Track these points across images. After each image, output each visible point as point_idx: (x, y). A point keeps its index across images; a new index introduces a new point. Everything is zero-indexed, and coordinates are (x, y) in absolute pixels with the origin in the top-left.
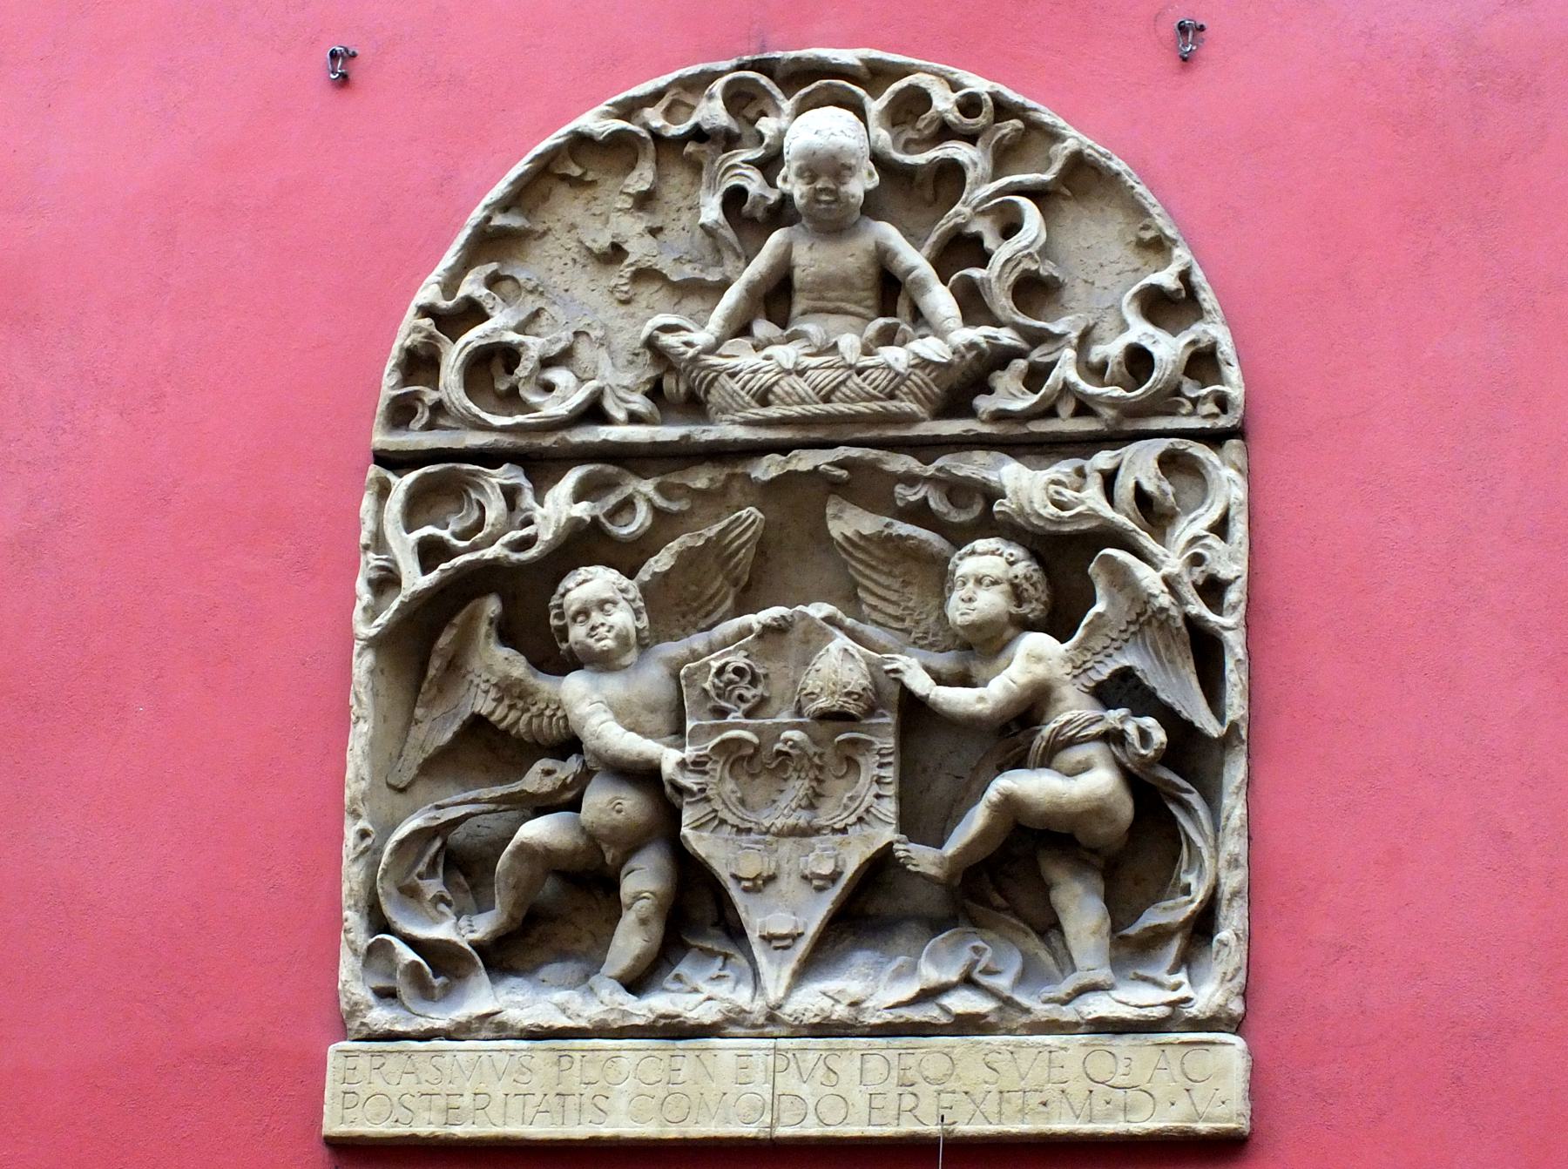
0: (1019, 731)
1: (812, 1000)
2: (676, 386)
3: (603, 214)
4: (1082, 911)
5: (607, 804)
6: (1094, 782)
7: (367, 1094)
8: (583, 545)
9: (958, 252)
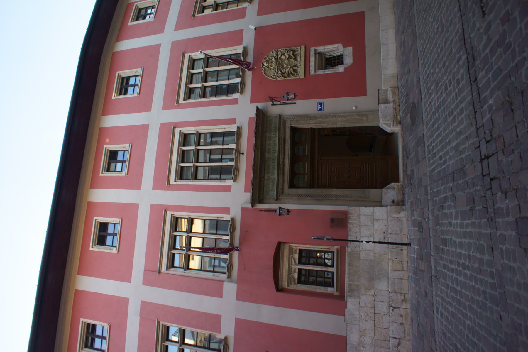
0: (289, 55)
1: (299, 60)
2: (274, 69)
3: (267, 73)
4: (296, 53)
5: (291, 69)
6: (291, 52)
7: (302, 76)
8: (281, 71)
9: (270, 60)
